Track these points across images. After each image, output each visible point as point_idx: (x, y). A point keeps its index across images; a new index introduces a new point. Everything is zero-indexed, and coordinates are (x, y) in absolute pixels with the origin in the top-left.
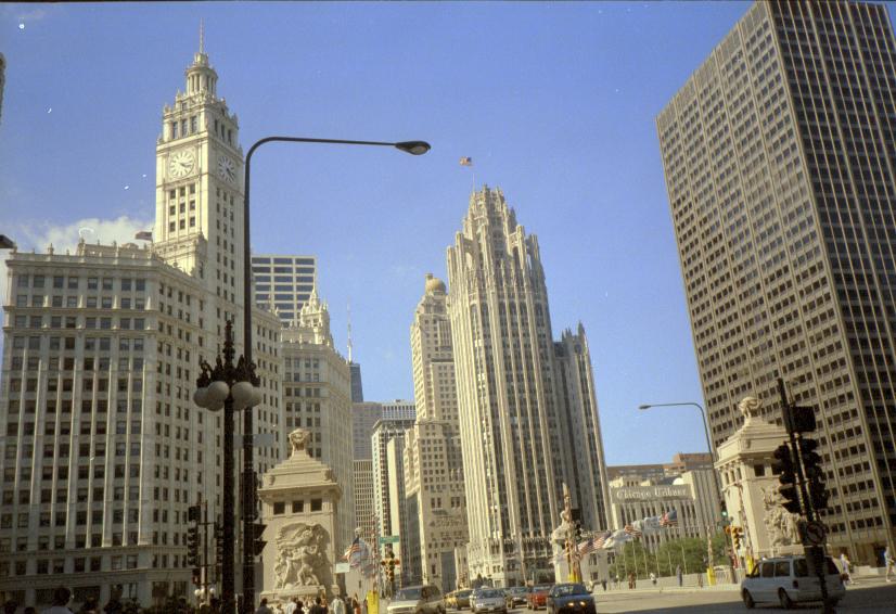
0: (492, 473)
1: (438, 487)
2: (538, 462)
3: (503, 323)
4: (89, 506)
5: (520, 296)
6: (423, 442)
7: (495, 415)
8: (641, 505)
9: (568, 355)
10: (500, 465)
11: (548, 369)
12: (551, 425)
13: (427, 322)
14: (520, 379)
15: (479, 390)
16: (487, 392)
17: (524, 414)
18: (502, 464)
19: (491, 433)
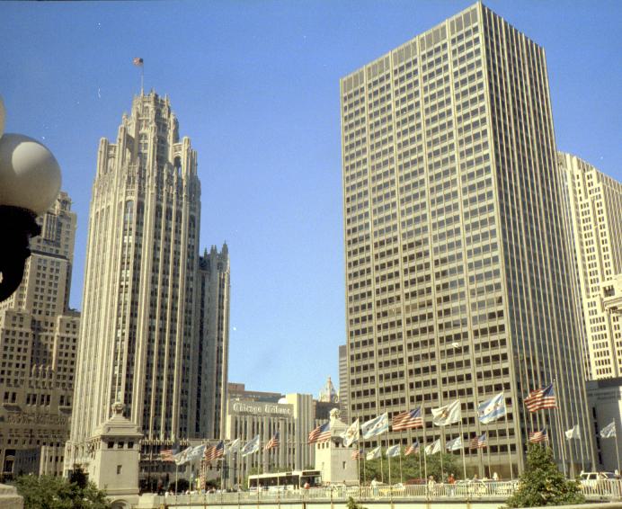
0: (120, 371)
1: (16, 381)
3: (157, 226)
5: (177, 204)
6: (8, 332)
7: (134, 315)
9: (210, 271)
10: (130, 363)
11: (192, 279)
14: (165, 283)
15: (121, 287)
16: (130, 289)
17: (163, 318)
19: (127, 331)
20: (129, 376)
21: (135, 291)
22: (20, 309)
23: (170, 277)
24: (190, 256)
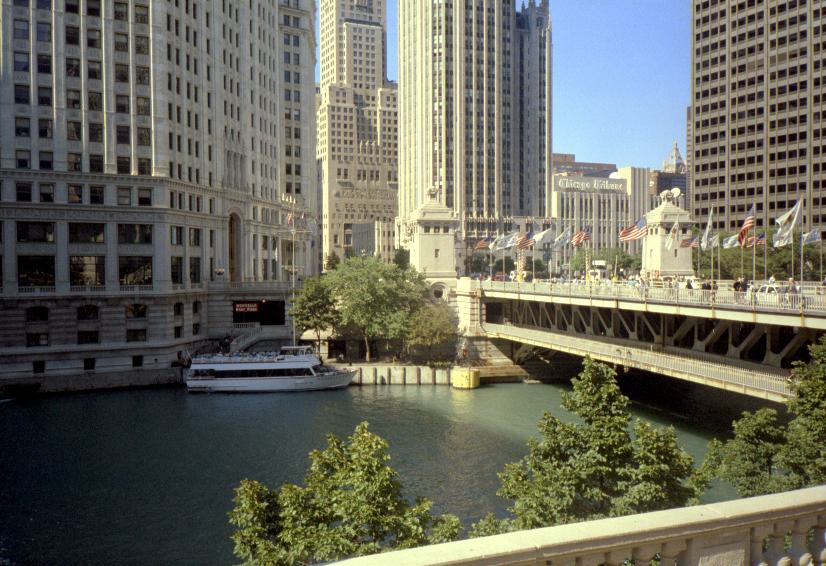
0: (440, 147)
1: (346, 158)
2: (489, 141)
4: (84, 114)
7: (449, 85)
8: (617, 197)
9: (529, 28)
10: (449, 139)
11: (509, 40)
12: (506, 104)
14: (480, 48)
15: (434, 55)
17: (480, 87)
18: (452, 139)
19: (443, 104)
20: (449, 152)
21: (449, 59)
22: (341, 84)
23: (485, 40)
24: (505, 13)
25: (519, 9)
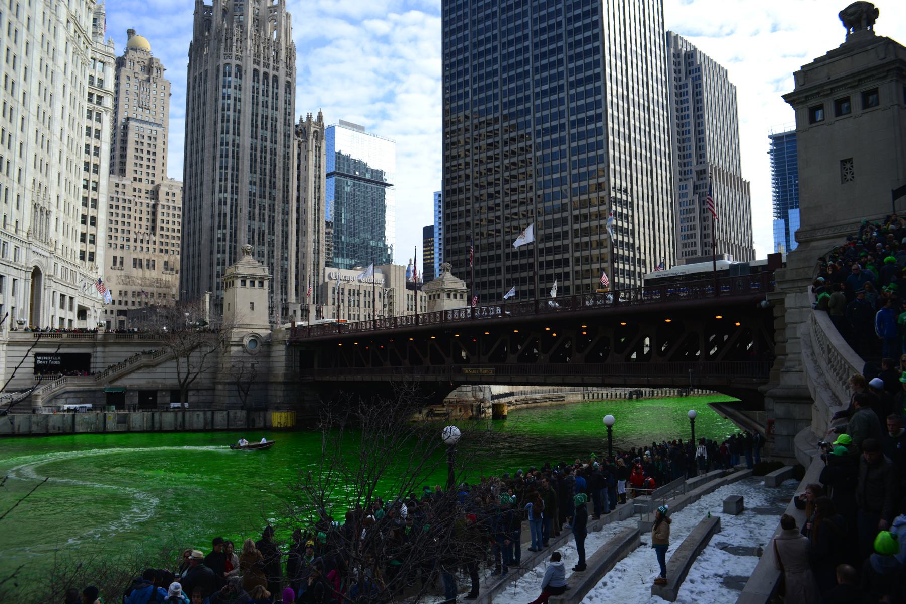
1: (122, 247)
13: (129, 77)
25: (297, 122)
